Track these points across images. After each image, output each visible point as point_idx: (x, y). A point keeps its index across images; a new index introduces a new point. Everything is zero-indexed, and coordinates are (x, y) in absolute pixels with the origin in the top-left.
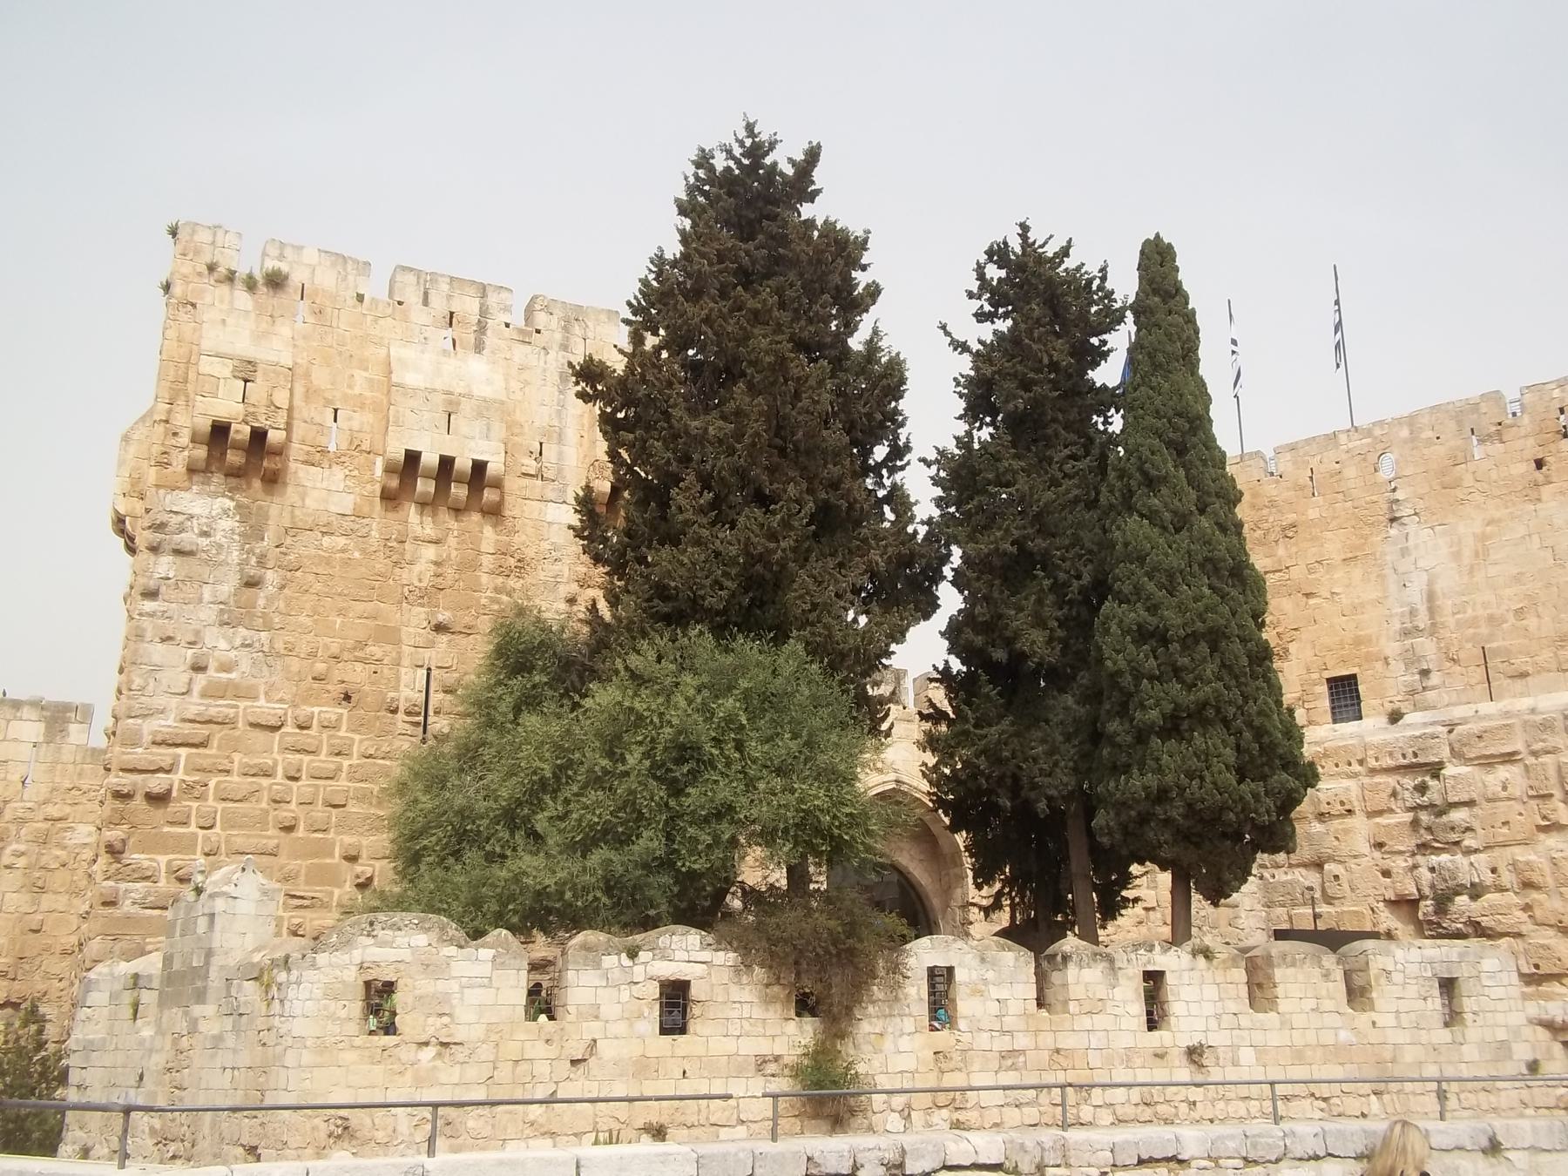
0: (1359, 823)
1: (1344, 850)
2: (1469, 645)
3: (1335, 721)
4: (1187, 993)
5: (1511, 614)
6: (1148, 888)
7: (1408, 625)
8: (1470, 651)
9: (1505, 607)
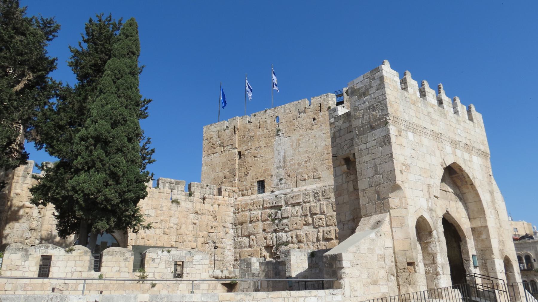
0: (260, 224)
1: (255, 231)
2: (293, 171)
3: (258, 193)
4: (59, 264)
6: (194, 242)
7: (278, 165)
8: (292, 173)
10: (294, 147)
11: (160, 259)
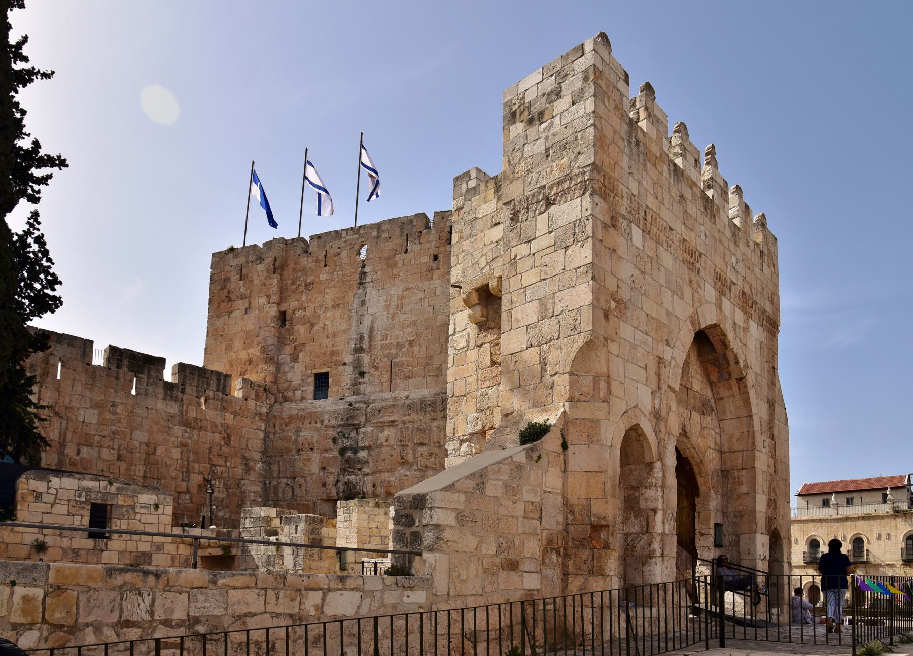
2: (385, 359)
3: (315, 399)
5: (408, 343)
9: (405, 339)
10: (391, 311)
11: (56, 495)
